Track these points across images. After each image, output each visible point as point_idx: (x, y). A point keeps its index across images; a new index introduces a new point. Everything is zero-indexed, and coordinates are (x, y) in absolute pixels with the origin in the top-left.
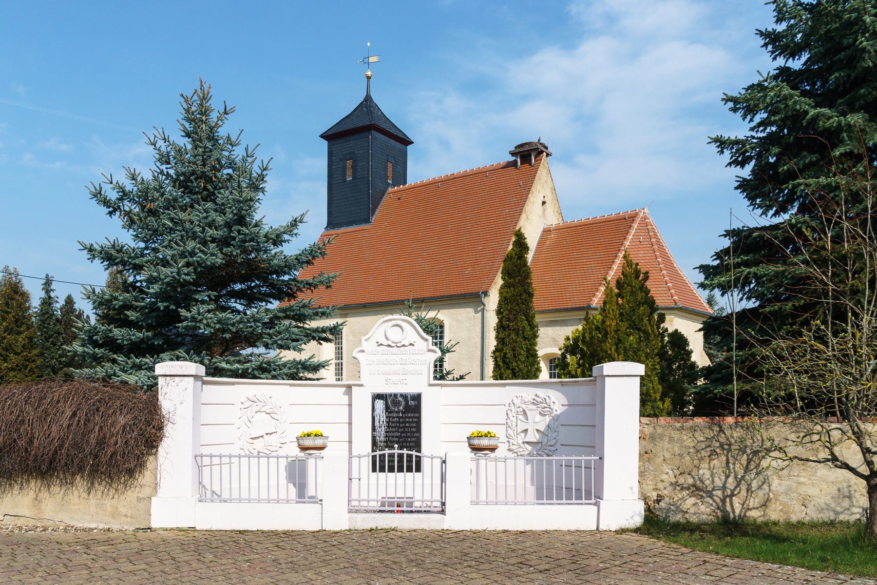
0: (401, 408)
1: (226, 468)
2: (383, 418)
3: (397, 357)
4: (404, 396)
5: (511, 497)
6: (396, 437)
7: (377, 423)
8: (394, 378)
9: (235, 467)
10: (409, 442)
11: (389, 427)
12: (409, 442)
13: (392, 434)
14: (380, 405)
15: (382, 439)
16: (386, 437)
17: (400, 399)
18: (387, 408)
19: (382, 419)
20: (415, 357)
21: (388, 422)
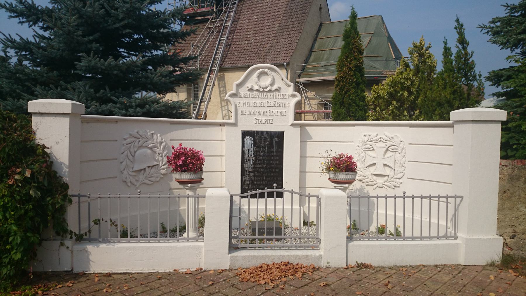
0: (267, 144)
1: (443, 205)
2: (252, 152)
3: (264, 101)
4: (269, 133)
5: (434, 203)
6: (263, 168)
7: (246, 156)
8: (262, 118)
9: (443, 205)
10: (273, 172)
11: (256, 159)
12: (273, 172)
13: (259, 166)
14: (249, 140)
15: (251, 170)
16: (254, 168)
17: (266, 136)
18: (255, 144)
19: (250, 153)
20: (280, 101)
21: (255, 156)
